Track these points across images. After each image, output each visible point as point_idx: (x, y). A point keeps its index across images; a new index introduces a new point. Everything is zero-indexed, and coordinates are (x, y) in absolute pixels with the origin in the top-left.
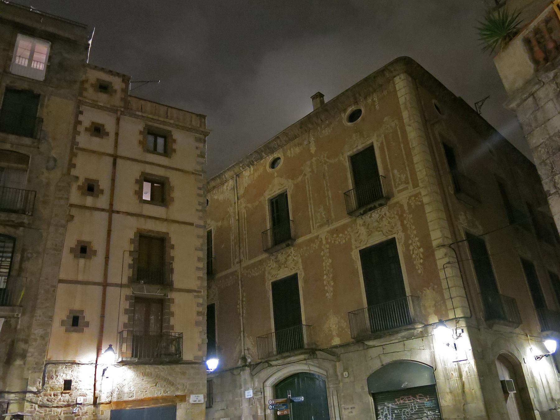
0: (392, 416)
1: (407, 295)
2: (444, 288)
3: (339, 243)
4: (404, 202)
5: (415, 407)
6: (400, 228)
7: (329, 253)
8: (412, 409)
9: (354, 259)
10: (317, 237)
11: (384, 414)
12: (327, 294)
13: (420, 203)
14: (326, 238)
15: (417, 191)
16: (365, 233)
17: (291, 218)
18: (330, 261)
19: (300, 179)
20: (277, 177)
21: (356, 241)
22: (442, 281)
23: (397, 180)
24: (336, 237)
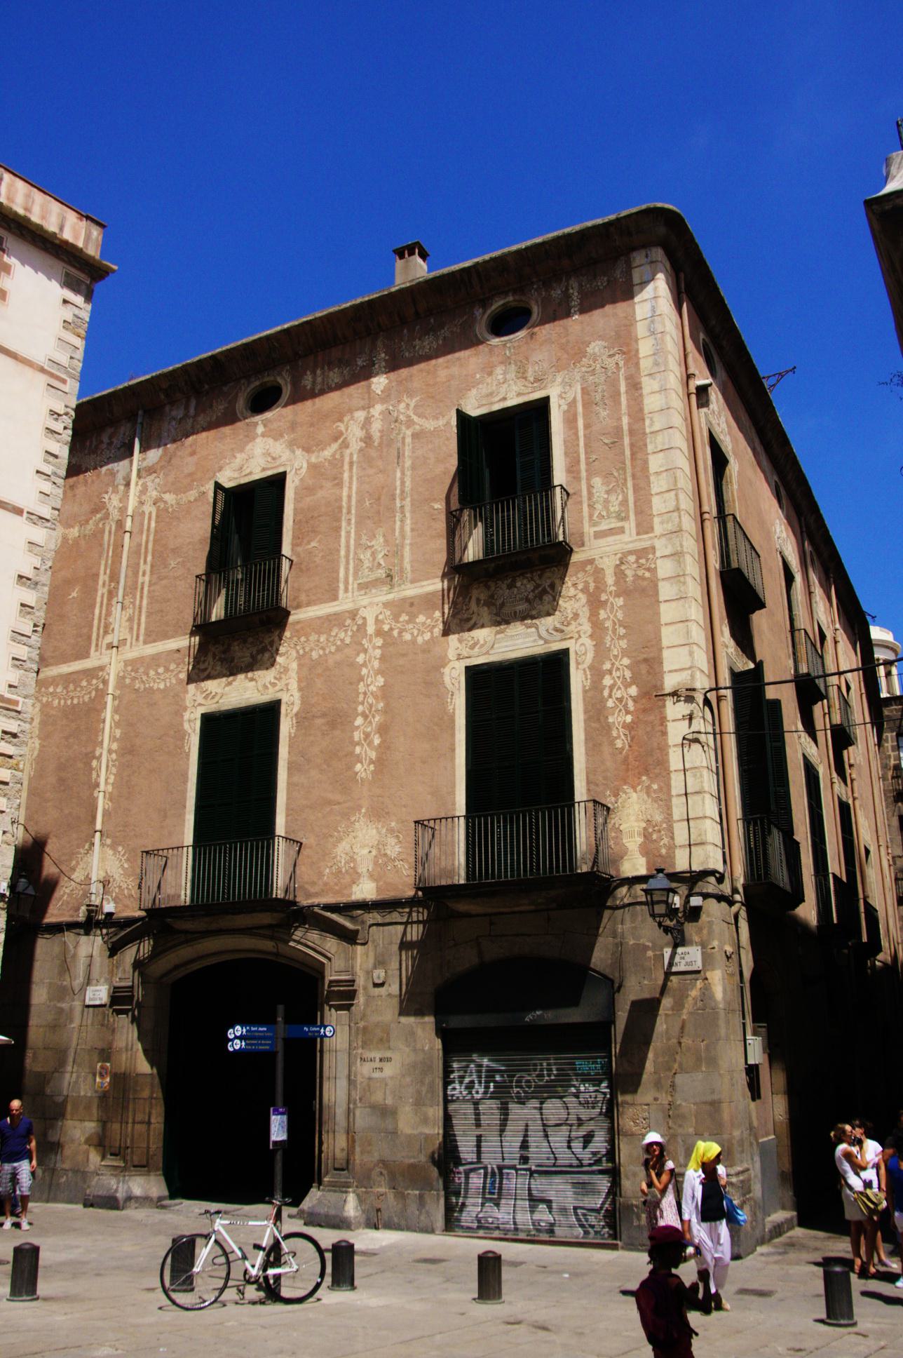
0: (487, 1087)
1: (577, 798)
2: (674, 792)
3: (414, 641)
4: (608, 565)
5: (551, 1070)
6: (587, 627)
7: (383, 659)
8: (541, 1076)
9: (449, 686)
10: (353, 614)
11: (467, 1080)
12: (358, 767)
14: (377, 619)
15: (647, 544)
17: (286, 549)
18: (380, 681)
19: (327, 453)
20: (263, 435)
22: (673, 776)
23: (598, 506)
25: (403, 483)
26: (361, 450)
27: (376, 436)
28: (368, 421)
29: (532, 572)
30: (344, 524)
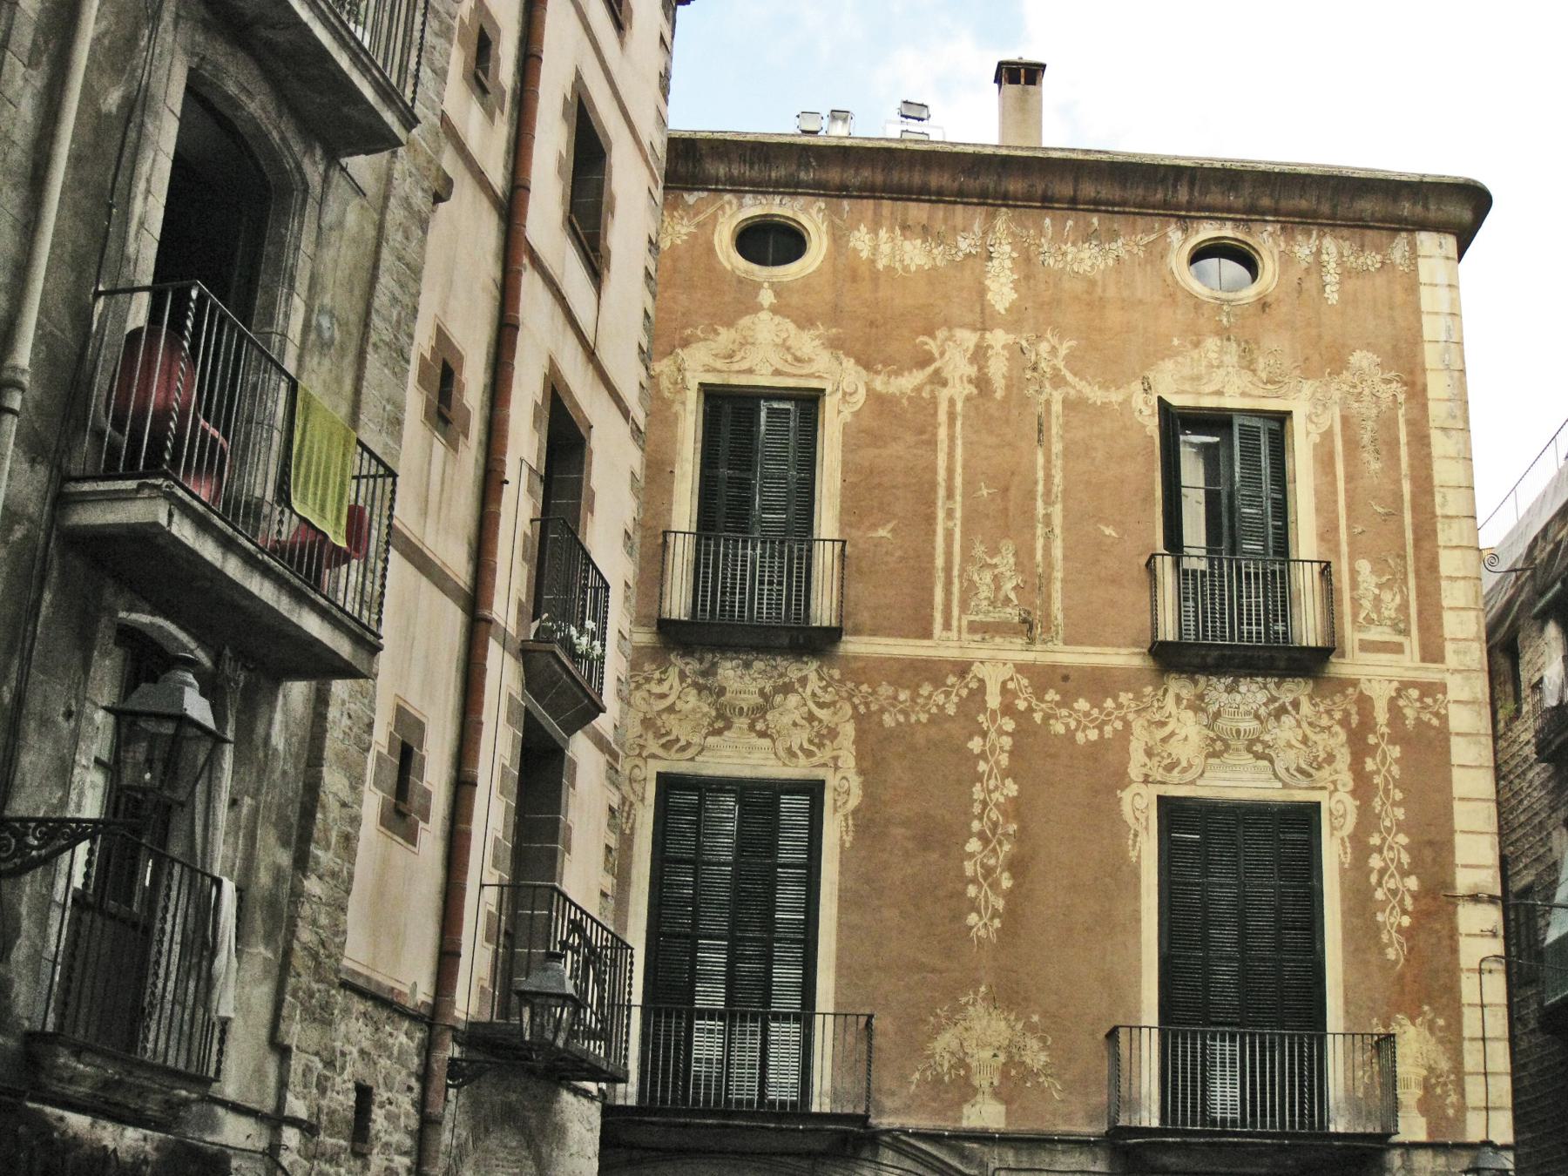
3: (1070, 735)
4: (1380, 694)
10: (963, 668)
13: (1435, 722)
18: (1012, 789)
21: (1149, 753)
23: (1367, 604)
24: (1058, 705)
25: (1048, 478)
26: (968, 399)
27: (999, 384)
28: (979, 355)
30: (941, 515)
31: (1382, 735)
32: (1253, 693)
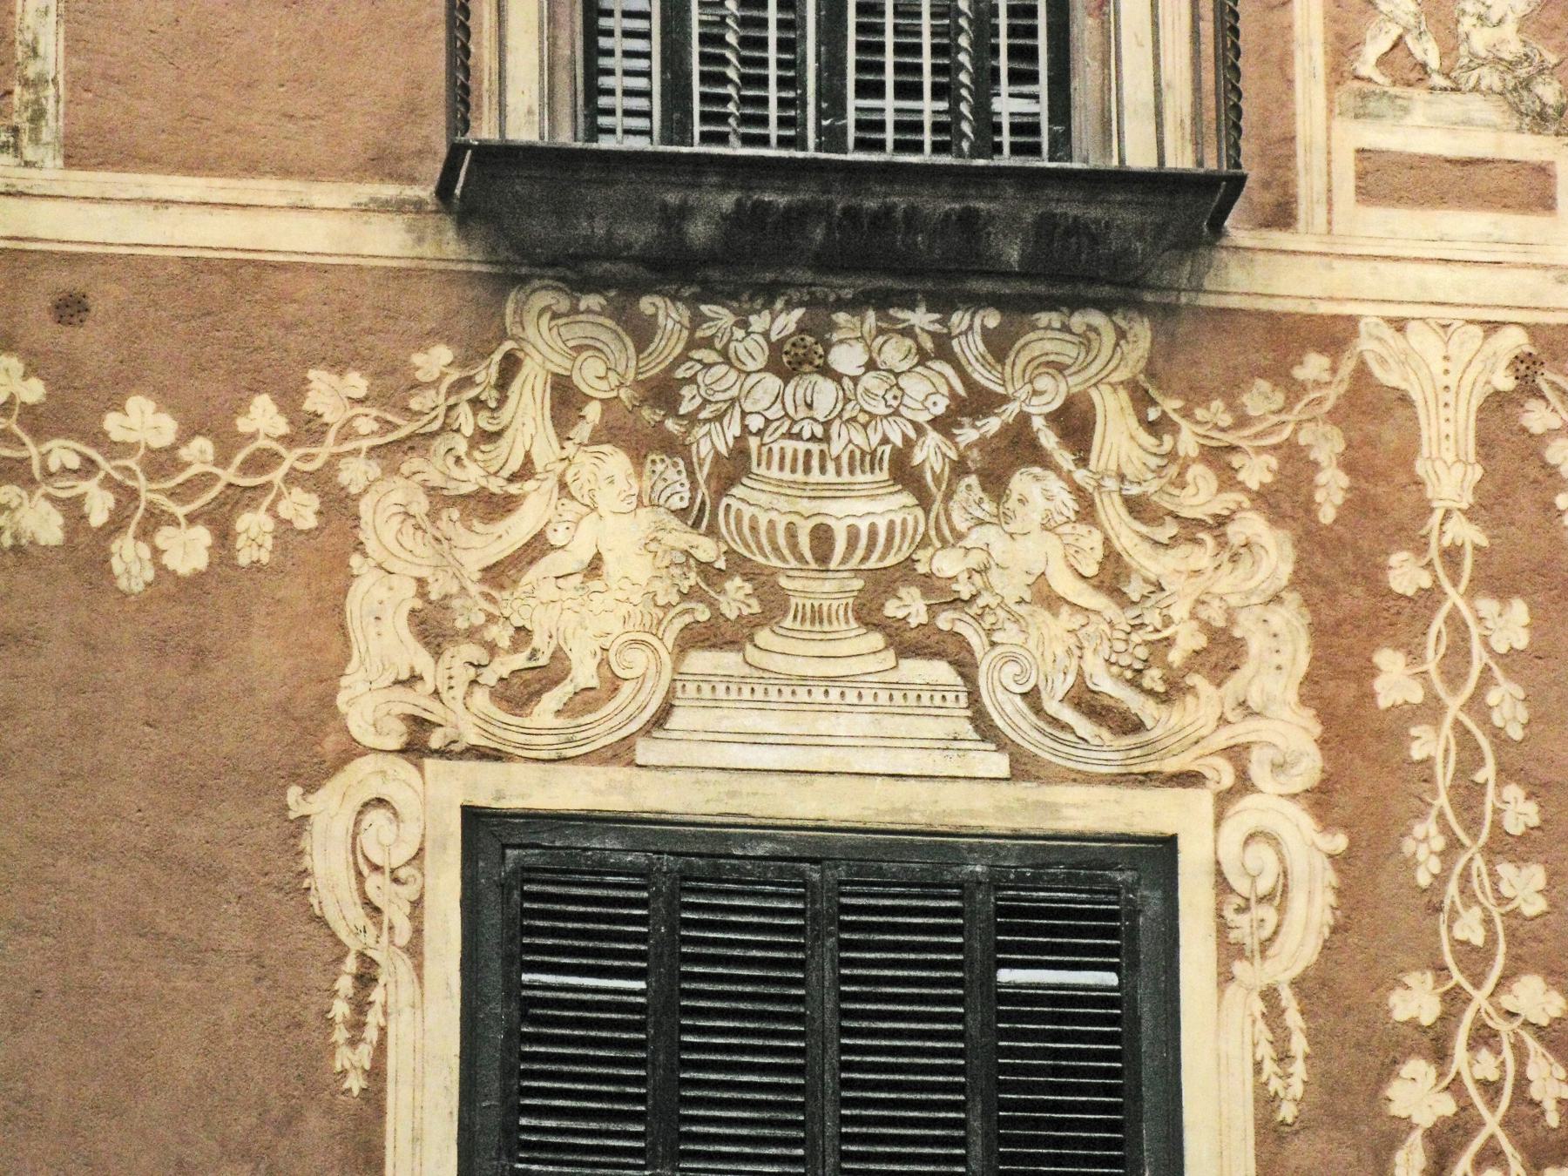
4: (1444, 382)
6: (1290, 738)
16: (631, 567)
21: (432, 628)
29: (943, 304)
31: (1452, 556)
32: (889, 373)
